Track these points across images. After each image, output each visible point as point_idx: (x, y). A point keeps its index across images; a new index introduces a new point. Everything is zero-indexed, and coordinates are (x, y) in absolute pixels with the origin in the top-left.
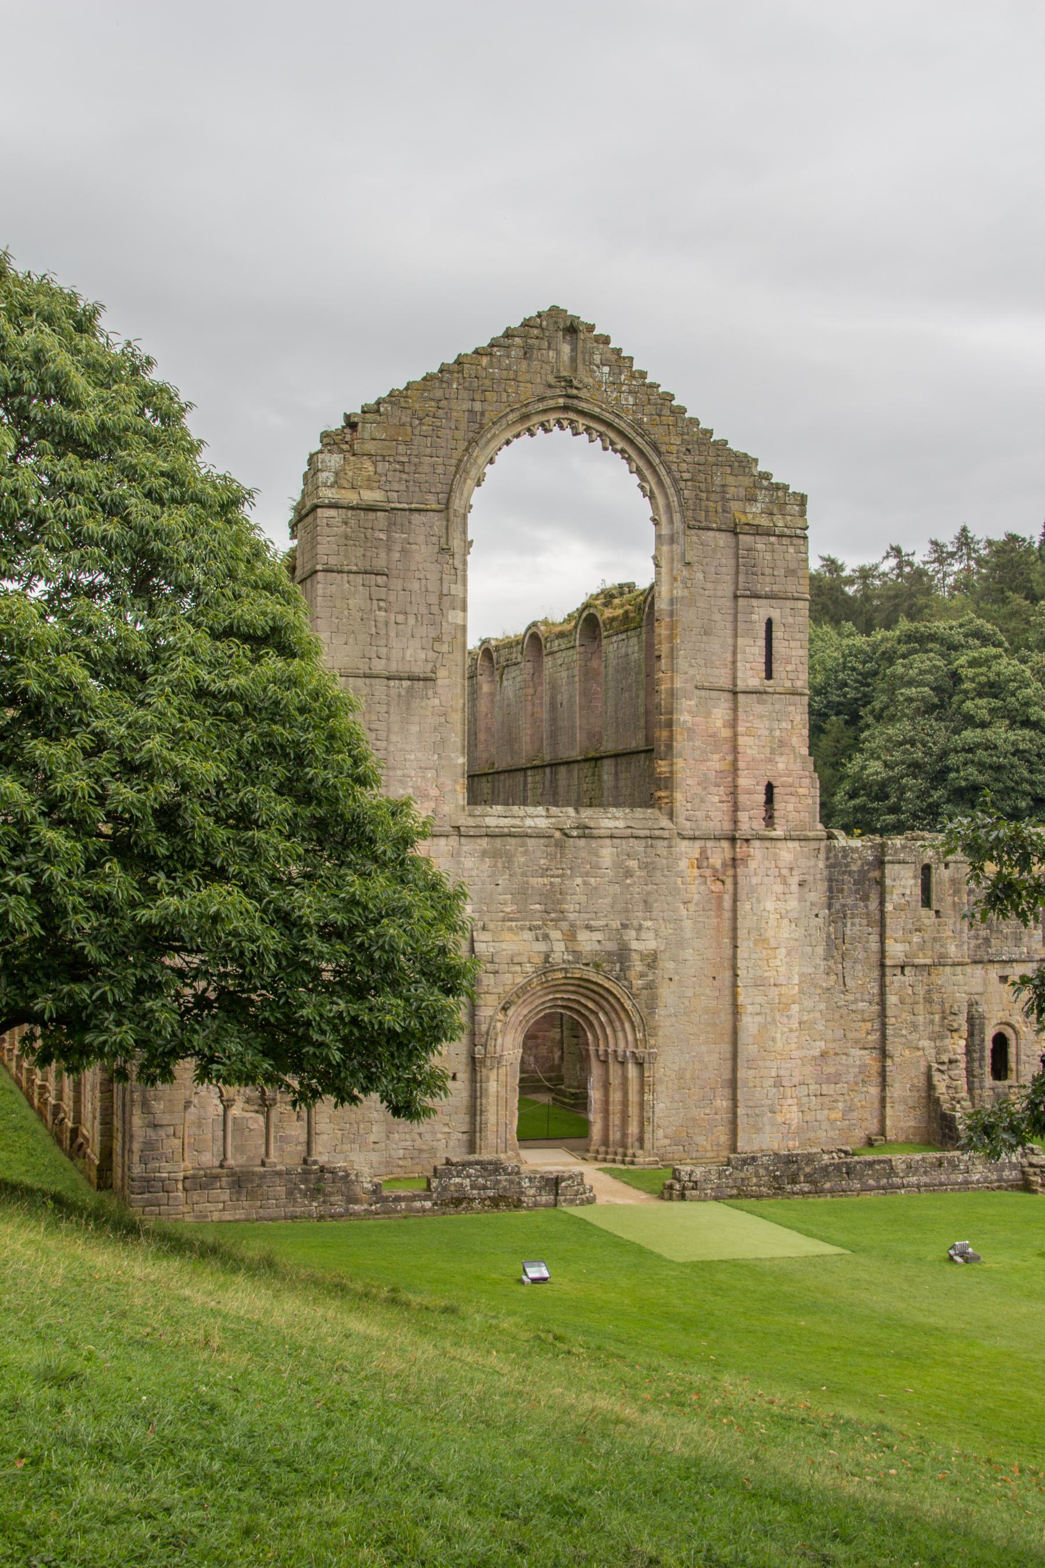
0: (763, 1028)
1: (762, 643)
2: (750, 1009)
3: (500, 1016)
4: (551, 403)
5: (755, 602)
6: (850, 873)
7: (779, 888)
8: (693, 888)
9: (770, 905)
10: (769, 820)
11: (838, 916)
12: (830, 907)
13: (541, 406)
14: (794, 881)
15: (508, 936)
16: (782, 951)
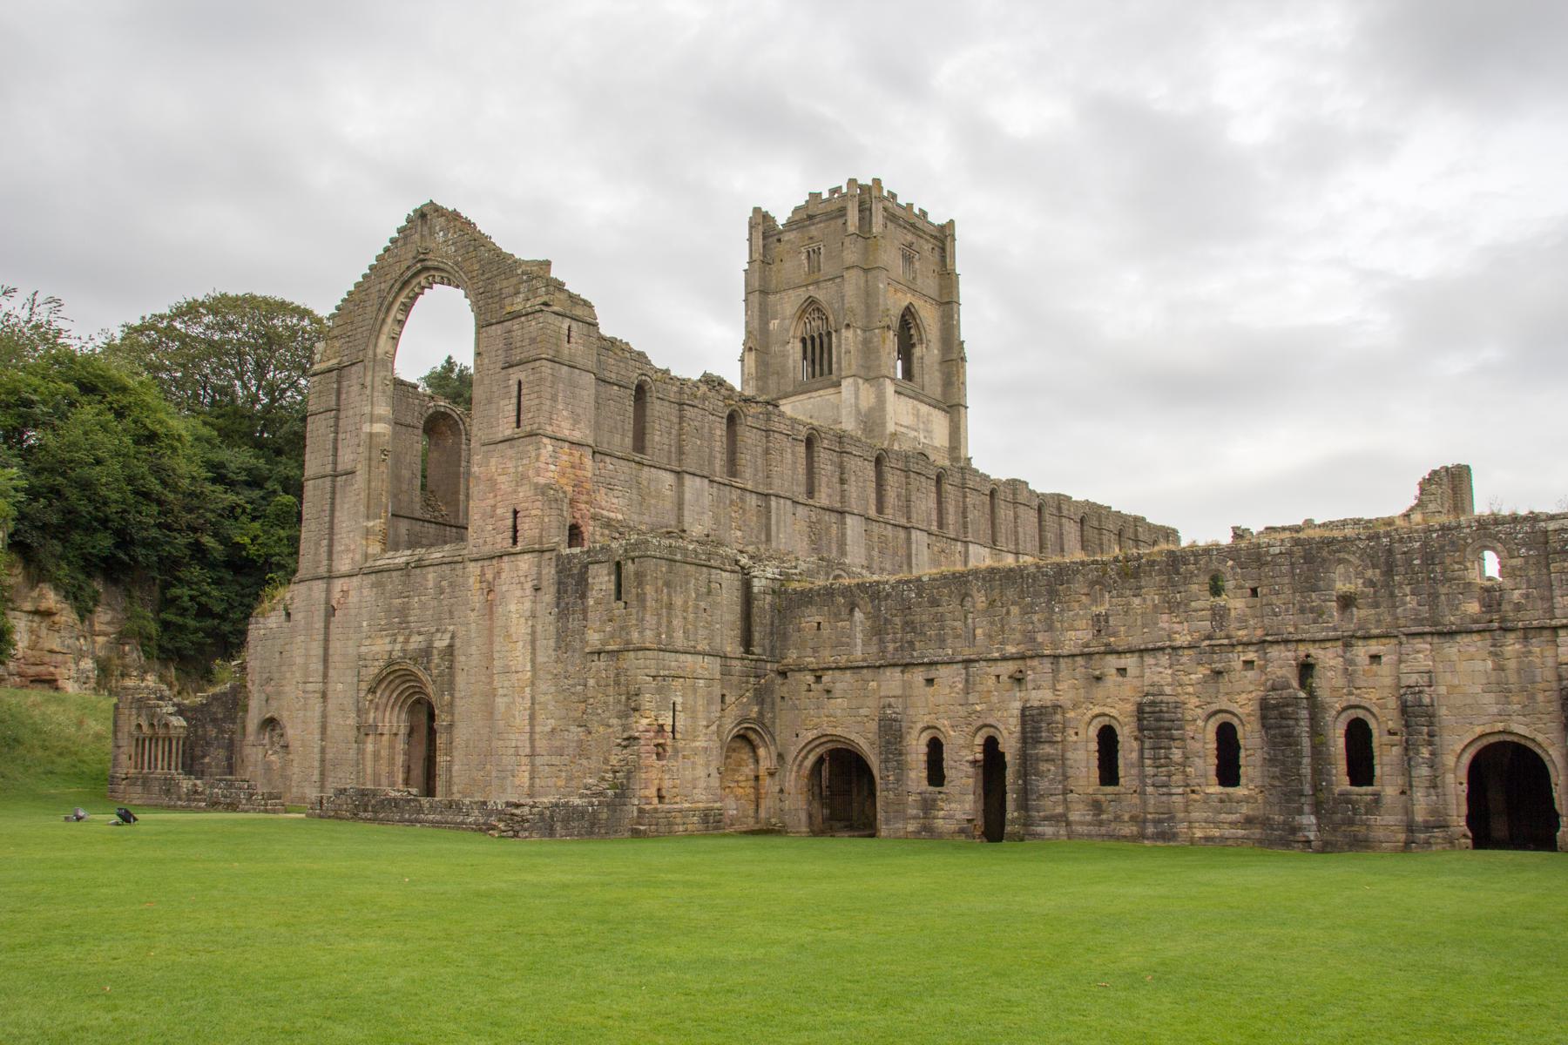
0: (508, 707)
1: (514, 401)
2: (501, 691)
3: (370, 697)
4: (414, 270)
5: (511, 370)
6: (572, 576)
7: (518, 593)
8: (476, 599)
9: (513, 607)
10: (515, 542)
11: (563, 614)
12: (558, 605)
13: (409, 274)
14: (528, 586)
15: (380, 641)
16: (521, 644)
